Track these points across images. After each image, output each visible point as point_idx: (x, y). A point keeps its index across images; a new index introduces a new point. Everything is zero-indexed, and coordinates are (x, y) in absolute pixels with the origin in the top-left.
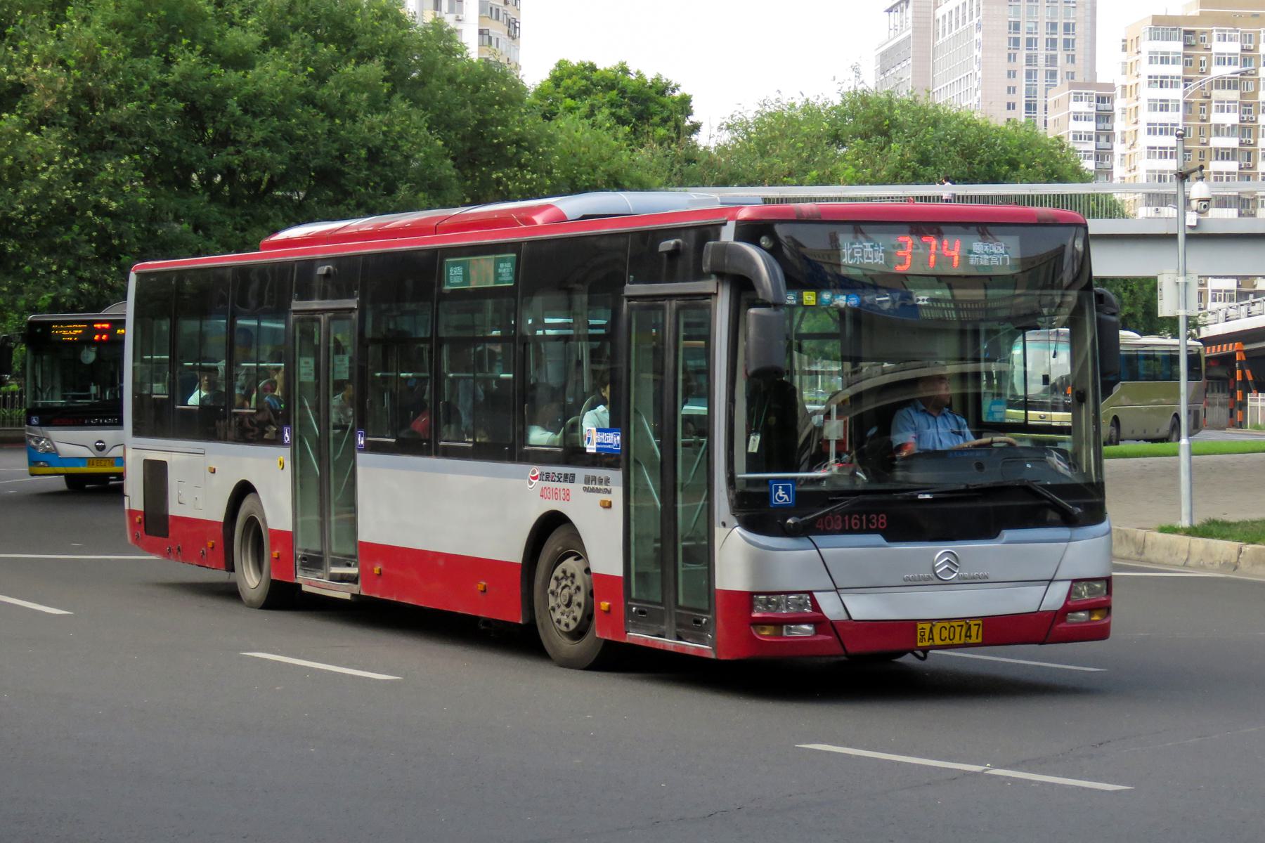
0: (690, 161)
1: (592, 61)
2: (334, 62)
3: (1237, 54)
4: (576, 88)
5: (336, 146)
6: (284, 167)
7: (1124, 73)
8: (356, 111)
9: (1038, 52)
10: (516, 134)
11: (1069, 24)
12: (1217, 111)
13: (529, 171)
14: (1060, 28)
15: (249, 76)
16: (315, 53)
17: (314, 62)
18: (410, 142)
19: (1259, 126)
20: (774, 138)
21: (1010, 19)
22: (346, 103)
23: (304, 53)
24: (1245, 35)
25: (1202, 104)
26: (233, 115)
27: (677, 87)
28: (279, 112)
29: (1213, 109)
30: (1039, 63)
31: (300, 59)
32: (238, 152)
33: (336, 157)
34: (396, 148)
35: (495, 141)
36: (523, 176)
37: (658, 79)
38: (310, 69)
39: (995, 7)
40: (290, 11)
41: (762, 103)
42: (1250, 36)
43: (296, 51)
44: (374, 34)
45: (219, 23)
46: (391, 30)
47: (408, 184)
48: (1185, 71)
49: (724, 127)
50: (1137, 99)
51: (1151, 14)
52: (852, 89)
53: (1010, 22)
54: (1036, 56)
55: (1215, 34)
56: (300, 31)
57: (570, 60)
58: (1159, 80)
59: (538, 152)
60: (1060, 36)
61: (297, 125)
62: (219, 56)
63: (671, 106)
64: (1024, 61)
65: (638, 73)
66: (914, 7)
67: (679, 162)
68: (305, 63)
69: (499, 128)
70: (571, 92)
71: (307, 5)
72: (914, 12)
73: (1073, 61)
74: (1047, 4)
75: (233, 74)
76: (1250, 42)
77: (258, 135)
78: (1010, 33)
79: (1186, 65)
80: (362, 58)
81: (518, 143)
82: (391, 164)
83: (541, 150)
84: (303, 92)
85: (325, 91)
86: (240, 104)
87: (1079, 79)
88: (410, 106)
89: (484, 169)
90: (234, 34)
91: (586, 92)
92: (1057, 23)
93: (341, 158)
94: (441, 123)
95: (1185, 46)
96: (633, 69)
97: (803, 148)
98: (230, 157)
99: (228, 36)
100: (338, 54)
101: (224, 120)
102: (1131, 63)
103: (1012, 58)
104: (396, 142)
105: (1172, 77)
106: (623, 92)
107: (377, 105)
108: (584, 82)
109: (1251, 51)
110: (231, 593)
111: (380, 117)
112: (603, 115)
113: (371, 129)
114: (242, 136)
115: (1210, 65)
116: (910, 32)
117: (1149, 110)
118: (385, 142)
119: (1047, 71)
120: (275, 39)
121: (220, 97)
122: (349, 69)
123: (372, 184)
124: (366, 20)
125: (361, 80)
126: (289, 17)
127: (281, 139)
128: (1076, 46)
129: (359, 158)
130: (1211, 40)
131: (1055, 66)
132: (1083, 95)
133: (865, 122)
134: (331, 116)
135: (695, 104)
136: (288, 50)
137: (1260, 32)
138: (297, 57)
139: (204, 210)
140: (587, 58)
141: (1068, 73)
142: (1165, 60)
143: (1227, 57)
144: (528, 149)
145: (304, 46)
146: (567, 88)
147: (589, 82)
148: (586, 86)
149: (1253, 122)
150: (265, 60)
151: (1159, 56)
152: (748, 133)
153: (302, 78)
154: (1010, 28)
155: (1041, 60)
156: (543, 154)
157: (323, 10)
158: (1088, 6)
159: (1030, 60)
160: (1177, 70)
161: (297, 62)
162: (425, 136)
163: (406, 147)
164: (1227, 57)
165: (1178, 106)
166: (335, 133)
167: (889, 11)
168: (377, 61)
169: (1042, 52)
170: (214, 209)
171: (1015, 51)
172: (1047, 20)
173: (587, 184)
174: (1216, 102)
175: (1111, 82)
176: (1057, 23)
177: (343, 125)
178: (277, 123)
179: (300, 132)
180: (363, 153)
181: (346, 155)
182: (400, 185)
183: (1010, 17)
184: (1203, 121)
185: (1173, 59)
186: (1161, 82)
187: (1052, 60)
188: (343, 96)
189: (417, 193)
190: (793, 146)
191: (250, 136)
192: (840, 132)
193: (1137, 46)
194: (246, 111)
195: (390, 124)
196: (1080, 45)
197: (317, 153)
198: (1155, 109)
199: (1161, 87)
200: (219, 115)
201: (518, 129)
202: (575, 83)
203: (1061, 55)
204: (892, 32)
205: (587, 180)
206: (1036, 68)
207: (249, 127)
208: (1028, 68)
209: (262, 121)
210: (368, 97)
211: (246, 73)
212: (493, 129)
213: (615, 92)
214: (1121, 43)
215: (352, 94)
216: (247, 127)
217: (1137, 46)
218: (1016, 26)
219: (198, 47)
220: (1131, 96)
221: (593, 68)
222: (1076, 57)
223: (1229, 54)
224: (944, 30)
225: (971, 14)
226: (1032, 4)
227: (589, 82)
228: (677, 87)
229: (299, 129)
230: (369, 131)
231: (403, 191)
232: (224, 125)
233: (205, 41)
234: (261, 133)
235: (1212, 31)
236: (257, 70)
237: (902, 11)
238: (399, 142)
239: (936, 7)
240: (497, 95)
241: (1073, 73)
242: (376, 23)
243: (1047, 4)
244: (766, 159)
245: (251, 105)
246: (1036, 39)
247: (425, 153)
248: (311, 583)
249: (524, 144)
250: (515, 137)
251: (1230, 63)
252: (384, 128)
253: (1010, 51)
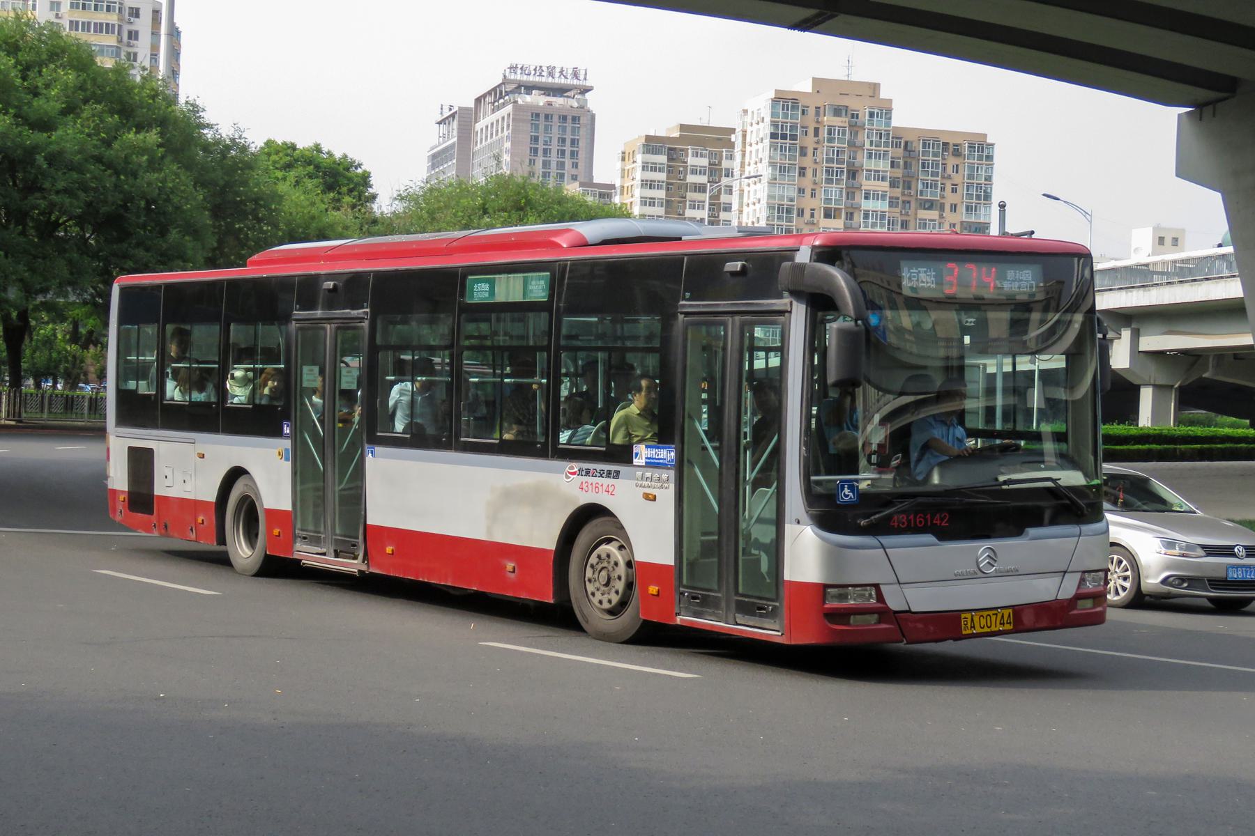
0: (375, 222)
1: (293, 141)
2: (117, 130)
3: (706, 167)
4: (282, 162)
5: (121, 196)
6: (81, 210)
7: (623, 177)
8: (137, 171)
9: (552, 159)
10: (254, 193)
11: (575, 139)
12: (690, 208)
13: (265, 224)
14: (568, 142)
15: (53, 137)
16: (102, 121)
17: (103, 128)
18: (179, 196)
19: (720, 220)
20: (439, 208)
21: (532, 134)
22: (130, 163)
23: (93, 121)
24: (712, 154)
25: (679, 202)
26: (40, 167)
27: (360, 165)
28: (71, 167)
29: (688, 207)
30: (552, 167)
31: (92, 125)
32: (44, 198)
33: (121, 206)
34: (168, 200)
35: (238, 199)
36: (261, 228)
37: (345, 156)
38: (103, 135)
39: (521, 124)
40: (82, 88)
41: (425, 181)
42: (716, 154)
43: (88, 119)
44: (149, 109)
45: (28, 94)
46: (163, 107)
47: (178, 229)
48: (667, 179)
49: (399, 198)
50: (632, 197)
51: (644, 134)
52: (493, 174)
53: (531, 136)
54: (550, 161)
55: (690, 151)
56: (91, 103)
57: (276, 140)
58: (649, 183)
59: (271, 209)
60: (568, 148)
61: (92, 178)
62: (27, 120)
63: (355, 180)
64: (541, 165)
65: (329, 153)
66: (459, 121)
67: (367, 223)
68: (97, 128)
69: (242, 189)
70: (278, 166)
71: (95, 84)
72: (459, 125)
73: (577, 167)
74: (559, 124)
75: (40, 133)
76: (715, 159)
77: (61, 185)
78: (531, 144)
79: (669, 172)
80: (140, 128)
81: (256, 201)
82: (164, 213)
83: (273, 207)
84: (96, 153)
85: (112, 152)
86: (46, 158)
87: (581, 178)
88: (179, 168)
89: (229, 220)
90: (41, 103)
91: (288, 166)
92: (565, 138)
93: (125, 207)
94: (200, 183)
95: (669, 160)
96: (325, 150)
97: (463, 217)
98: (38, 202)
99: (35, 104)
100: (120, 124)
101: (33, 171)
102: (628, 170)
103: (532, 162)
104: (168, 196)
105: (659, 182)
106: (317, 167)
107: (154, 165)
108: (289, 158)
109: (716, 165)
110: (222, 560)
111: (156, 175)
112: (310, 183)
113: (149, 184)
114: (47, 185)
115: (686, 174)
116: (455, 139)
117: (641, 205)
118: (159, 194)
119: (557, 173)
120: (70, 110)
121: (32, 151)
122: (131, 136)
123: (149, 228)
124: (142, 97)
125: (141, 145)
126: (80, 92)
127: (78, 189)
128: (580, 156)
129: (139, 207)
130: (687, 156)
131: (564, 169)
132: (590, 192)
133: (507, 200)
134: (117, 173)
135: (373, 180)
136: (79, 117)
137: (723, 151)
138: (89, 124)
139: (15, 241)
140: (289, 140)
141: (572, 176)
142: (653, 169)
143: (698, 168)
144: (264, 206)
145: (93, 116)
146: (275, 162)
147: (292, 159)
148: (290, 161)
149: (716, 217)
150: (66, 125)
151: (650, 165)
152: (417, 203)
153: (95, 142)
154: (531, 140)
155: (554, 165)
156: (274, 211)
157: (108, 89)
158: (589, 127)
159: (546, 164)
160: (662, 176)
161: (89, 127)
162: (191, 192)
163: (176, 200)
164: (698, 168)
165: (662, 203)
166: (120, 187)
167: (439, 123)
168: (154, 130)
169: (554, 158)
170: (22, 239)
171: (534, 158)
172: (559, 136)
173: (303, 236)
174: (690, 201)
175: (608, 182)
176: (565, 138)
177: (124, 180)
178: (76, 176)
179: (94, 185)
180: (143, 203)
181: (129, 205)
182: (171, 230)
183: (531, 132)
184: (680, 215)
185: (660, 168)
186: (651, 185)
187: (561, 165)
188: (126, 157)
189: (184, 236)
190: (455, 215)
191: (53, 185)
192: (487, 207)
193: (633, 157)
194: (50, 164)
195: (164, 181)
196: (582, 155)
197: (105, 202)
198: (645, 205)
199: (650, 188)
200: (29, 167)
201: (256, 189)
202: (281, 158)
203: (568, 162)
204: (441, 139)
205: (302, 233)
206: (549, 171)
207: (54, 179)
208: (544, 170)
209: (62, 174)
210: (147, 159)
211: (52, 134)
212: (237, 189)
213: (312, 167)
214: (621, 155)
215: (134, 156)
216: (52, 177)
217: (633, 157)
218: (536, 139)
219: (11, 111)
220: (627, 194)
221: (293, 147)
222: (579, 164)
223: (700, 167)
224: (481, 140)
225: (503, 128)
226: (548, 123)
227: (292, 159)
228: (360, 165)
229: (92, 182)
230: (148, 186)
231: (174, 235)
232: (33, 175)
233: (16, 107)
234: (63, 183)
235: (688, 149)
236: (60, 132)
237: (449, 124)
238: (171, 196)
239: (476, 122)
240: (239, 163)
241: (576, 176)
242: (151, 101)
243: (559, 124)
244: (436, 224)
245: (52, 159)
246: (550, 149)
247: (191, 204)
248: (308, 554)
249: (262, 203)
250: (253, 196)
251: (700, 173)
252: (160, 185)
253: (531, 157)
